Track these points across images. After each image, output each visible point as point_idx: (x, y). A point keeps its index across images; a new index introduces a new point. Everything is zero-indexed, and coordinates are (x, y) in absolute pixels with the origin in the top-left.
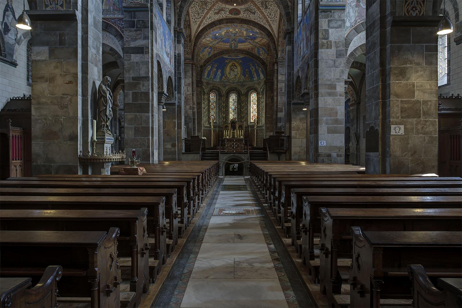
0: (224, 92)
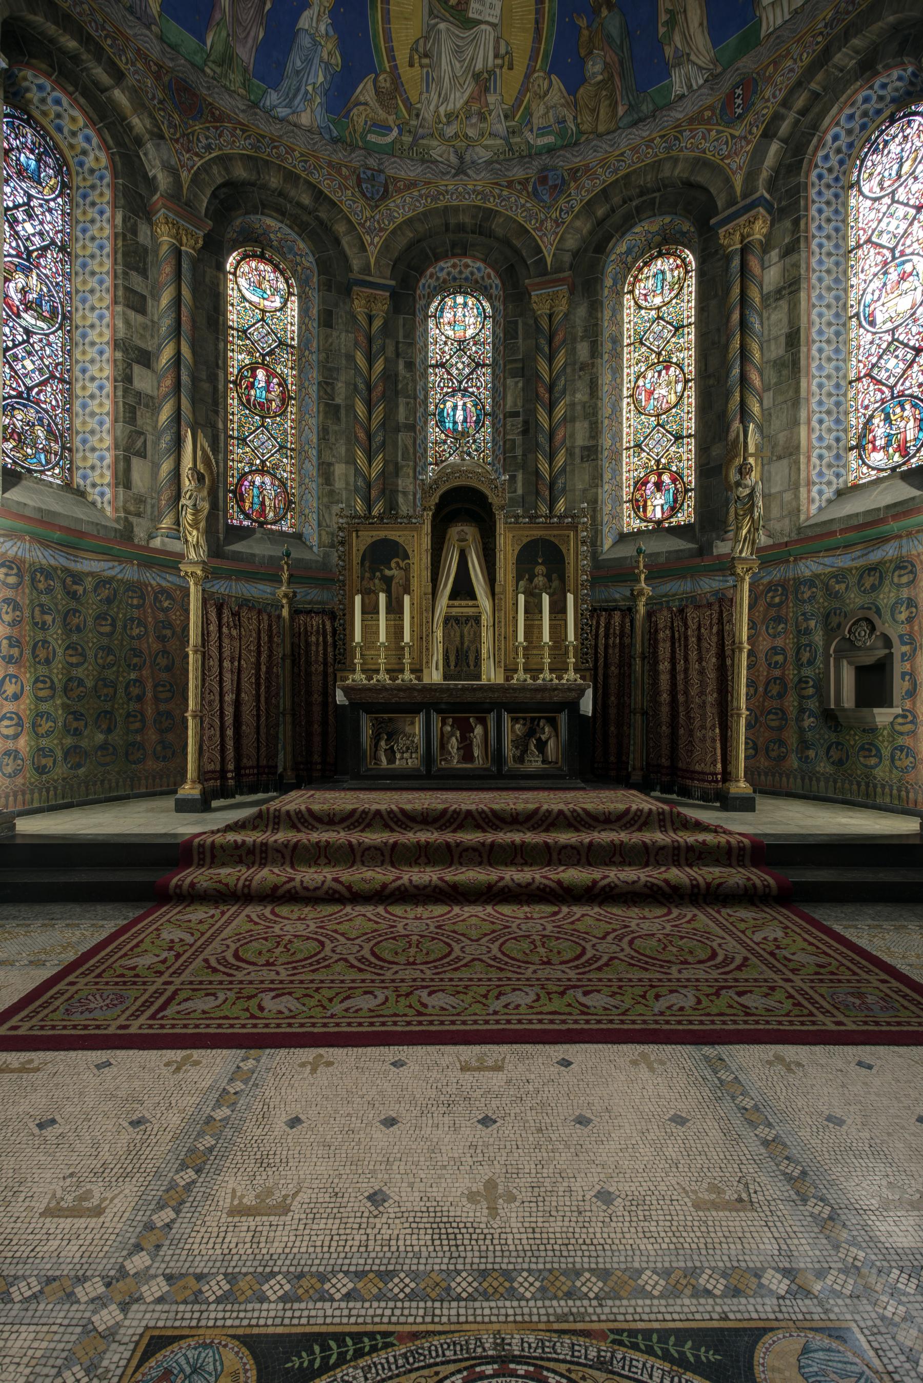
0: (374, 244)
